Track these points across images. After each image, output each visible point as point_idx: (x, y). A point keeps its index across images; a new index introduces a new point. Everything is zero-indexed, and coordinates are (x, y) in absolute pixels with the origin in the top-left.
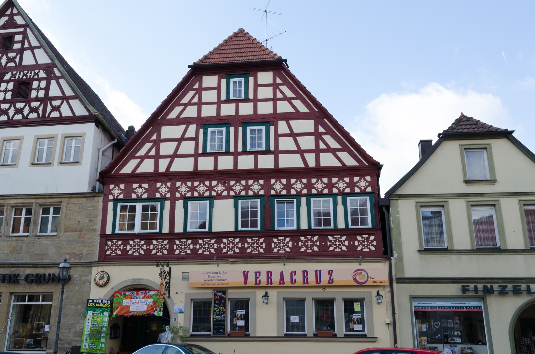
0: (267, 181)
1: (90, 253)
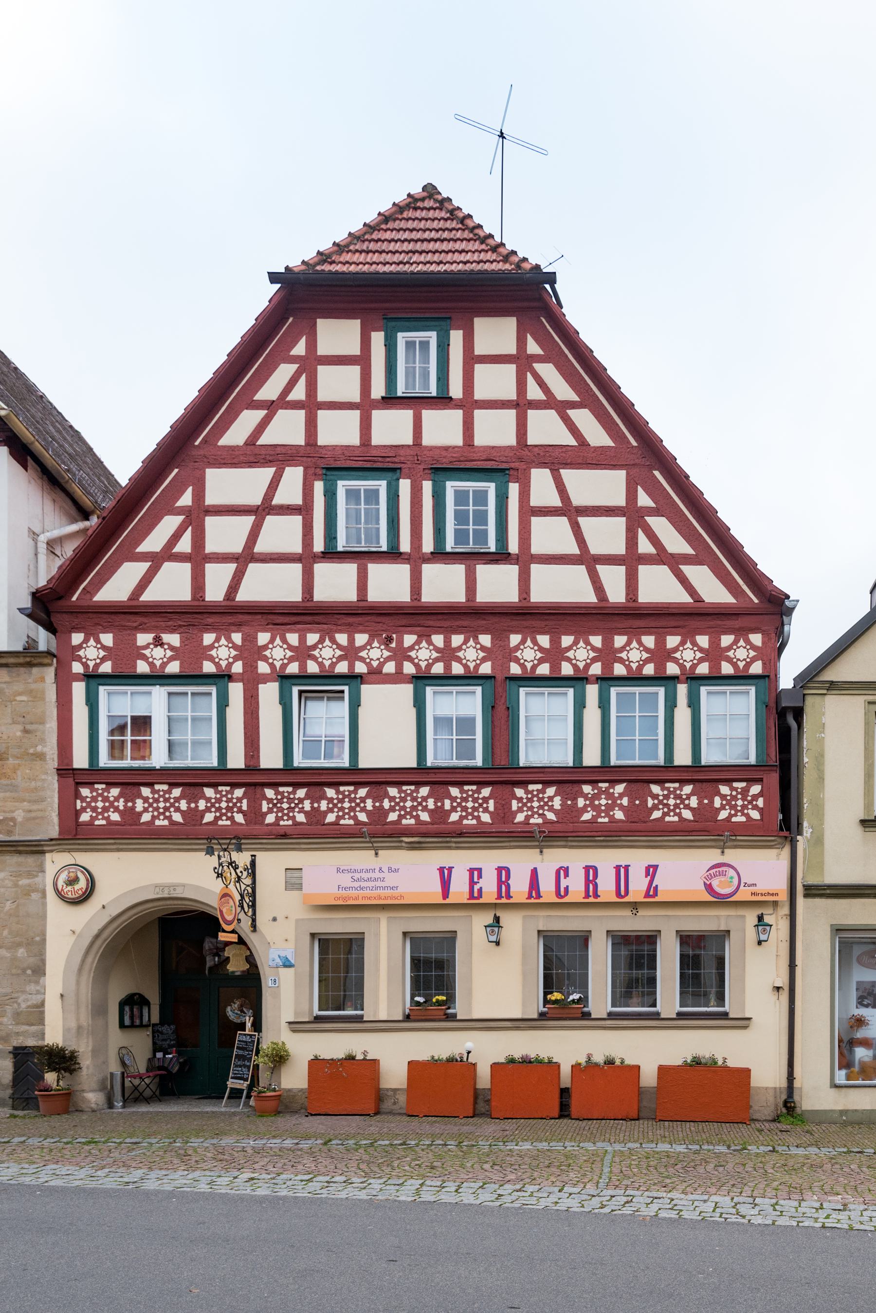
0: (500, 637)
1: (34, 818)
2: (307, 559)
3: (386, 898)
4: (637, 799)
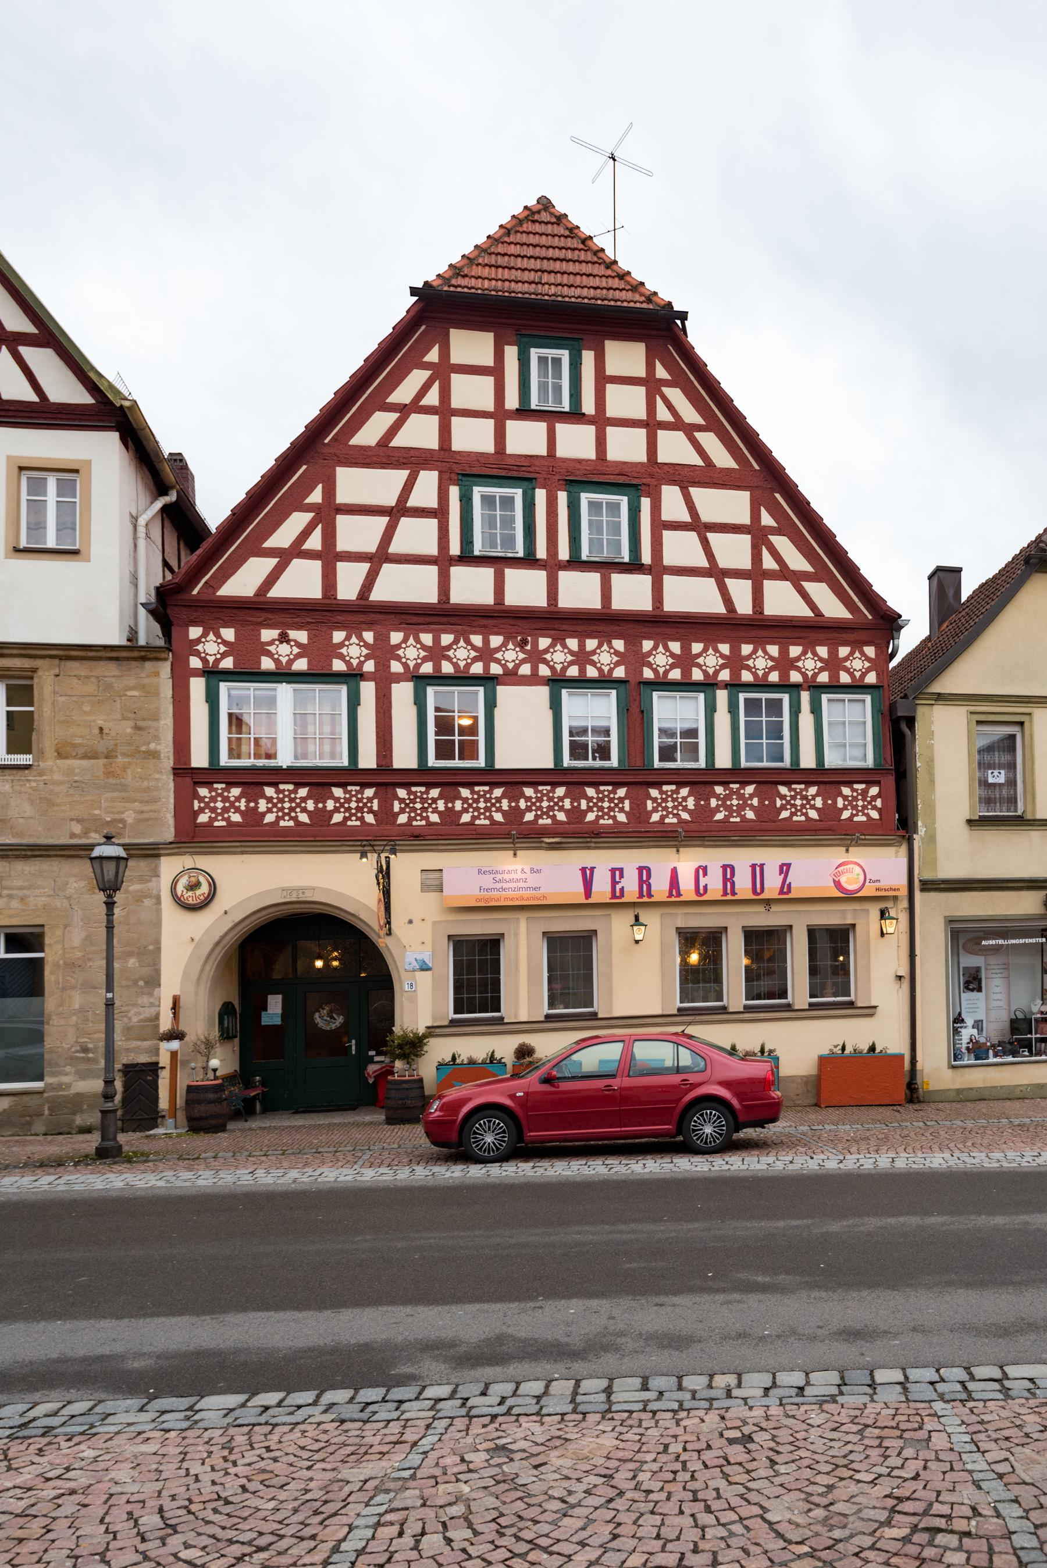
0: (633, 643)
1: (147, 820)
2: (443, 562)
3: (528, 899)
4: (766, 799)
